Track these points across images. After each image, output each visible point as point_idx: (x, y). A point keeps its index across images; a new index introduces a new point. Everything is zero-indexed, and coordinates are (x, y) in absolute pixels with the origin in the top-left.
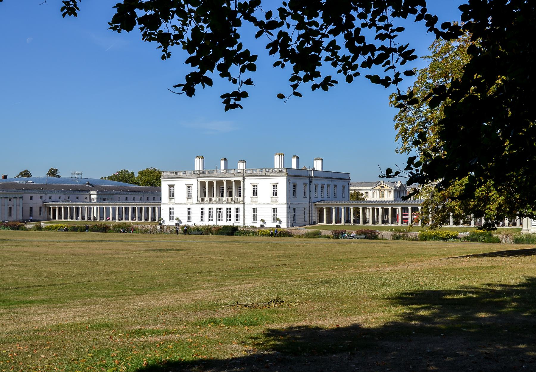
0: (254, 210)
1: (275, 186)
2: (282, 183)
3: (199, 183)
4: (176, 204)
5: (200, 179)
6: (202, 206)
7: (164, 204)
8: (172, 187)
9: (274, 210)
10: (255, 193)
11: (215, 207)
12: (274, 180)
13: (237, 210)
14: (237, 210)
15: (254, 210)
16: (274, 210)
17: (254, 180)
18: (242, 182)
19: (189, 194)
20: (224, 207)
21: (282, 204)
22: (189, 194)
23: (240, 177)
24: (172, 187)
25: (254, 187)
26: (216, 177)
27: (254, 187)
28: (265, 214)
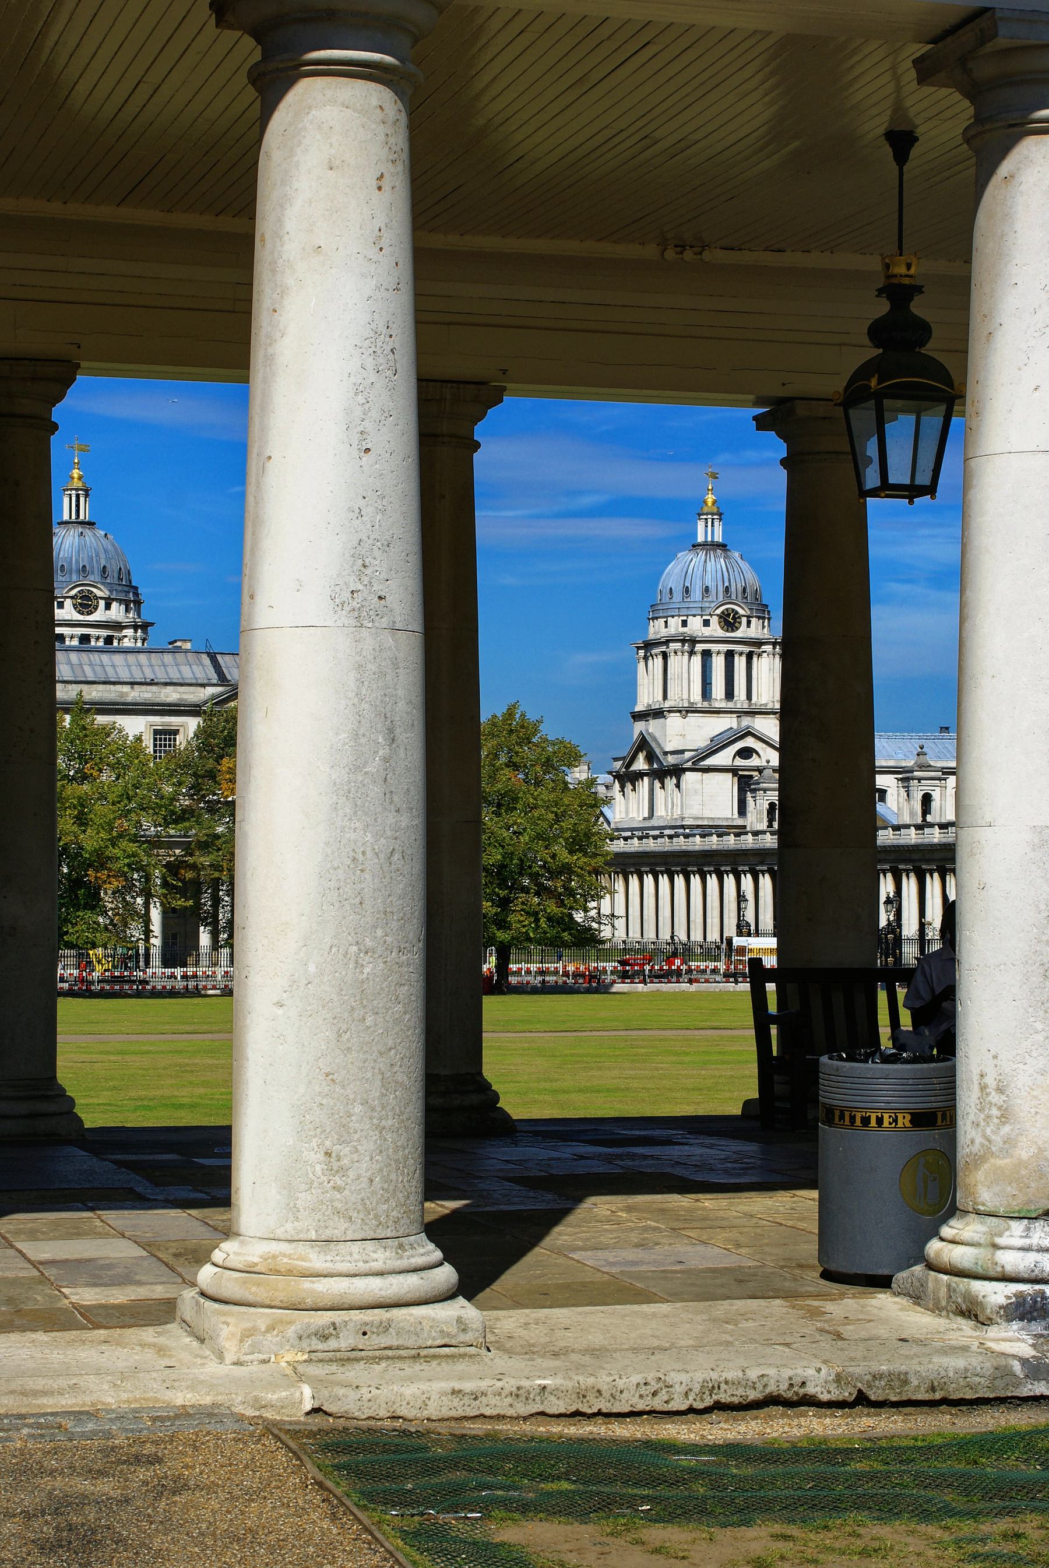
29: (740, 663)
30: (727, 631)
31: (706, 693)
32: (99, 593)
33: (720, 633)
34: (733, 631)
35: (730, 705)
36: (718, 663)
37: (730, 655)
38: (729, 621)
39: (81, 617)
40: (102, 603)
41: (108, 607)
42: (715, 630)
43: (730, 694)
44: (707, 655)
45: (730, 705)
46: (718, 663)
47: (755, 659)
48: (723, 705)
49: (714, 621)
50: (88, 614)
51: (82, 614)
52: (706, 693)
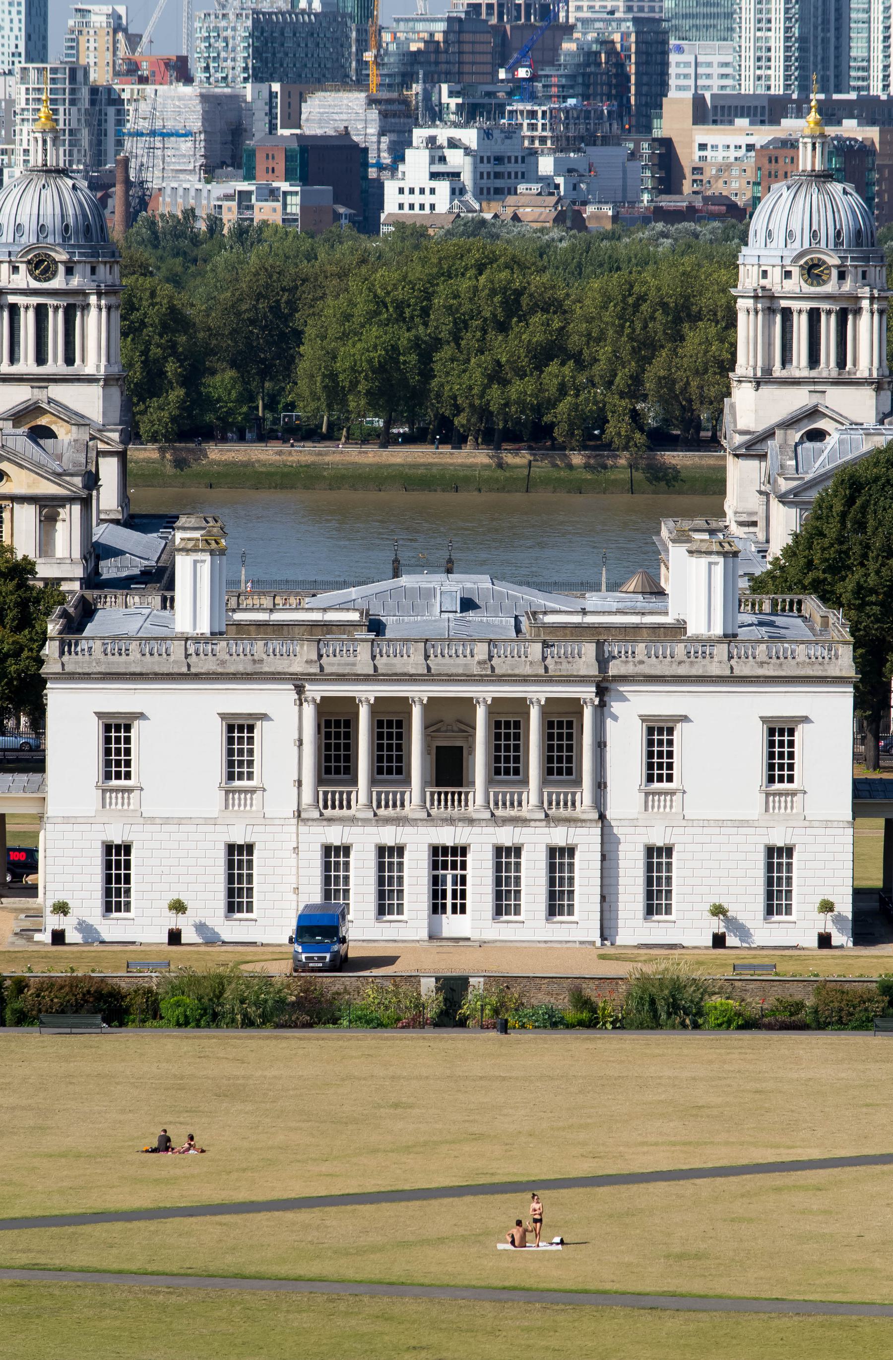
0: (657, 857)
1: (780, 736)
3: (309, 711)
4: (152, 820)
5: (316, 691)
6: (335, 835)
7: (67, 820)
8: (116, 733)
9: (778, 858)
10: (658, 763)
11: (417, 843)
12: (783, 703)
13: (560, 858)
14: (560, 858)
15: (657, 857)
16: (778, 858)
18: (588, 714)
20: (481, 844)
21: (827, 824)
23: (582, 680)
24: (116, 733)
25: (659, 736)
26: (429, 677)
27: (659, 736)
28: (716, 880)
29: (828, 327)
30: (812, 285)
31: (786, 360)
32: (58, 257)
33: (808, 289)
34: (819, 285)
35: (814, 373)
36: (801, 325)
37: (814, 316)
38: (813, 271)
39: (35, 284)
40: (61, 269)
41: (69, 271)
42: (796, 284)
43: (814, 360)
44: (787, 314)
45: (814, 373)
46: (801, 325)
47: (850, 317)
48: (805, 373)
49: (796, 271)
50: (46, 281)
51: (39, 280)
52: (786, 360)
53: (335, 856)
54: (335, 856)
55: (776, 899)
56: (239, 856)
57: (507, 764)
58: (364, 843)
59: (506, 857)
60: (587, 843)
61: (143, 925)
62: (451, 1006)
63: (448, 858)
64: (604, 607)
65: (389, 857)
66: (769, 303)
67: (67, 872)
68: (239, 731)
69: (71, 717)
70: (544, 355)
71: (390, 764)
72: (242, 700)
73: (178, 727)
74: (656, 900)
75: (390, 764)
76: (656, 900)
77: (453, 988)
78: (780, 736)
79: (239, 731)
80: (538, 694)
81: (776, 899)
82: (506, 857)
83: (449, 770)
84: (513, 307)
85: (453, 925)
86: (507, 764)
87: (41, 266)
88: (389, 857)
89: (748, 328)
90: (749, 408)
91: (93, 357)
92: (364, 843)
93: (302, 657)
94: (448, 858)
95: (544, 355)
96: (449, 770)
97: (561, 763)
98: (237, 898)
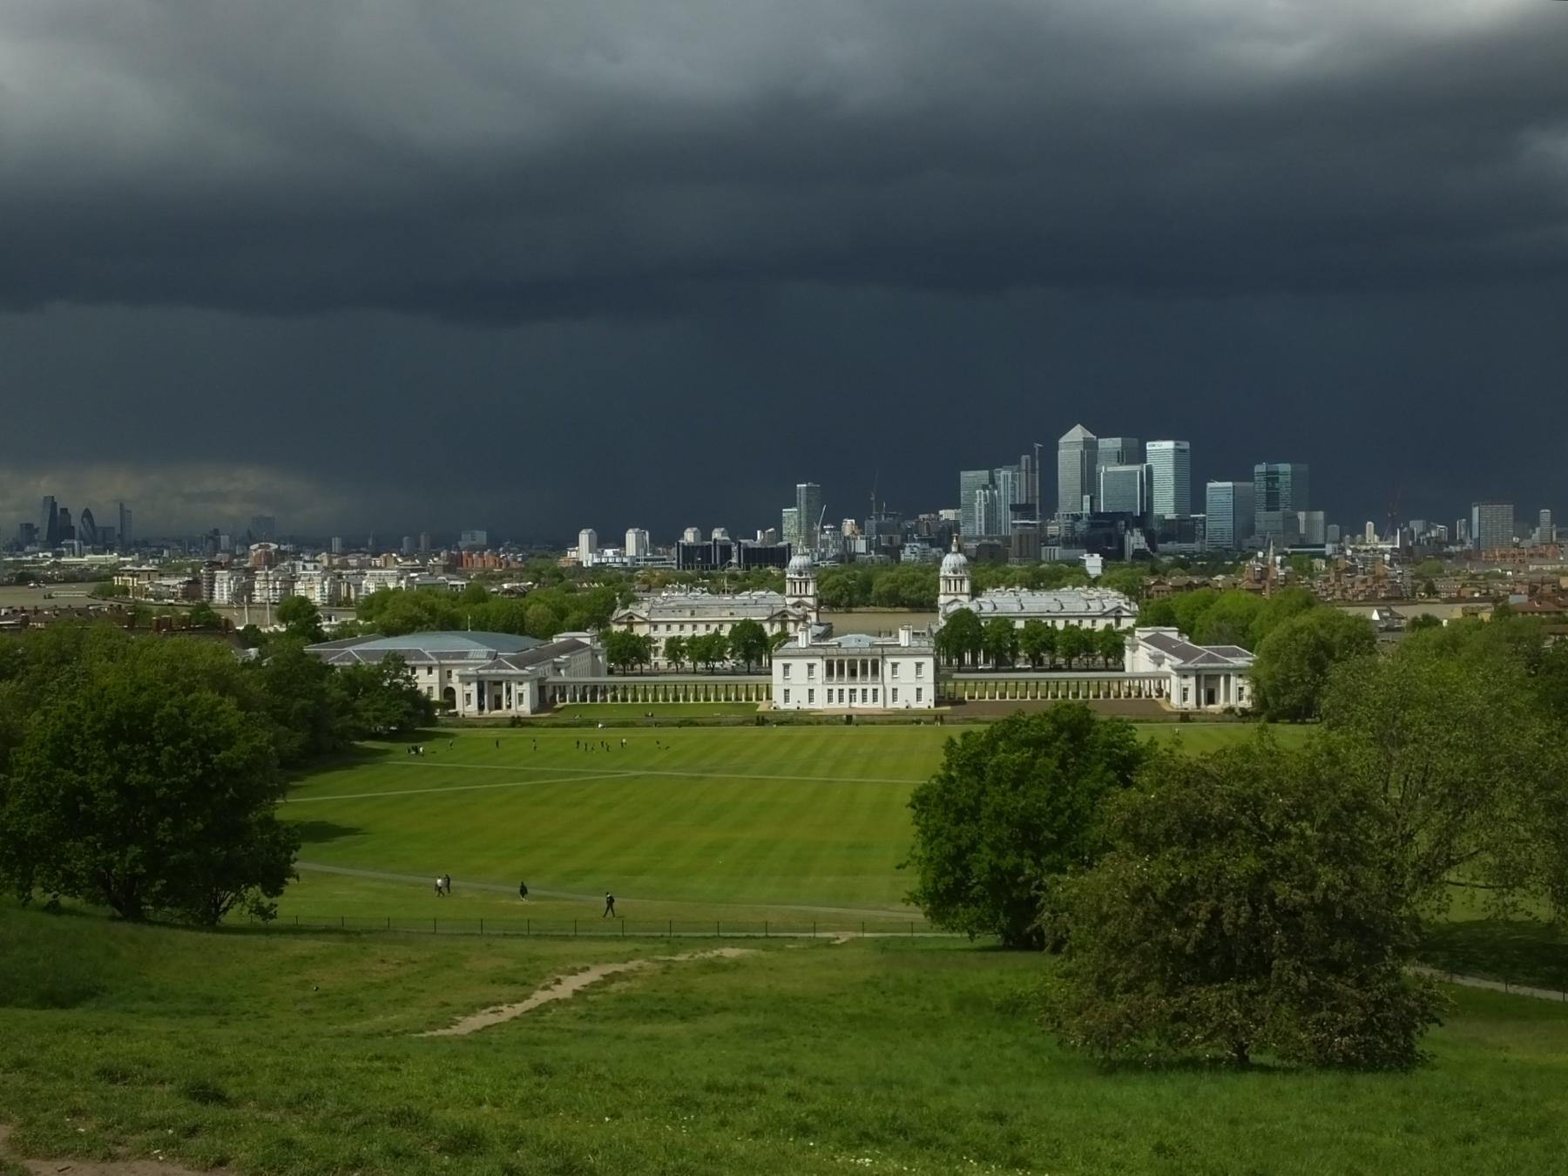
0: (895, 690)
1: (919, 665)
2: (929, 663)
8: (786, 666)
9: (919, 690)
10: (894, 672)
11: (846, 689)
13: (875, 691)
14: (875, 691)
15: (895, 690)
17: (895, 660)
19: (810, 673)
20: (859, 688)
22: (810, 673)
24: (786, 666)
25: (895, 665)
27: (895, 665)
38: (955, 572)
53: (830, 691)
54: (830, 691)
55: (919, 698)
56: (811, 691)
57: (864, 672)
58: (836, 689)
59: (864, 691)
60: (880, 688)
61: (791, 705)
62: (849, 720)
63: (853, 691)
64: (887, 640)
65: (841, 691)
66: (946, 578)
67: (778, 695)
68: (811, 666)
69: (777, 665)
70: (920, 589)
71: (841, 672)
72: (811, 661)
73: (799, 666)
74: (895, 698)
75: (841, 672)
76: (895, 698)
77: (849, 717)
78: (919, 665)
79: (811, 666)
80: (870, 659)
81: (919, 698)
82: (864, 691)
83: (853, 673)
84: (915, 580)
85: (854, 705)
86: (864, 672)
87: (800, 574)
88: (841, 691)
89: (942, 583)
90: (942, 599)
91: (811, 592)
92: (836, 689)
93: (821, 651)
94: (853, 691)
95: (920, 589)
96: (853, 673)
97: (875, 672)
98: (811, 699)
